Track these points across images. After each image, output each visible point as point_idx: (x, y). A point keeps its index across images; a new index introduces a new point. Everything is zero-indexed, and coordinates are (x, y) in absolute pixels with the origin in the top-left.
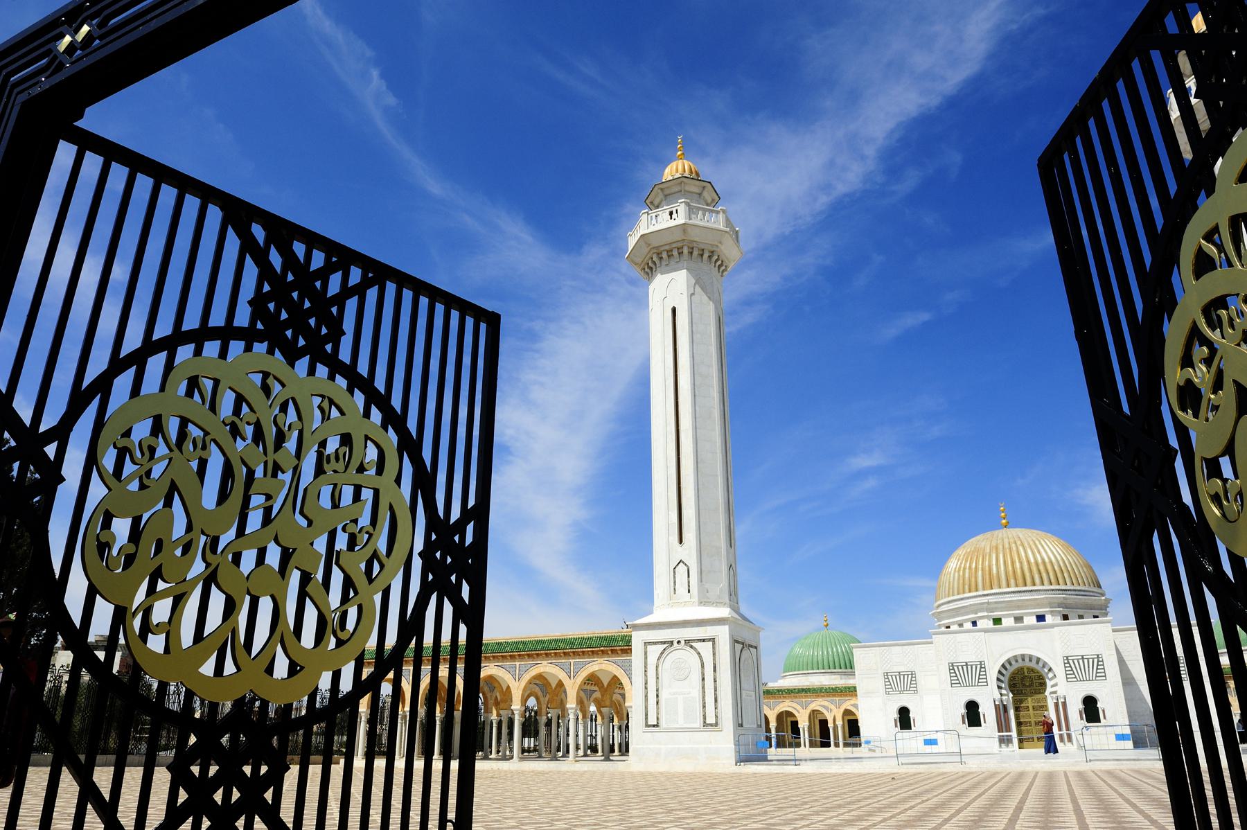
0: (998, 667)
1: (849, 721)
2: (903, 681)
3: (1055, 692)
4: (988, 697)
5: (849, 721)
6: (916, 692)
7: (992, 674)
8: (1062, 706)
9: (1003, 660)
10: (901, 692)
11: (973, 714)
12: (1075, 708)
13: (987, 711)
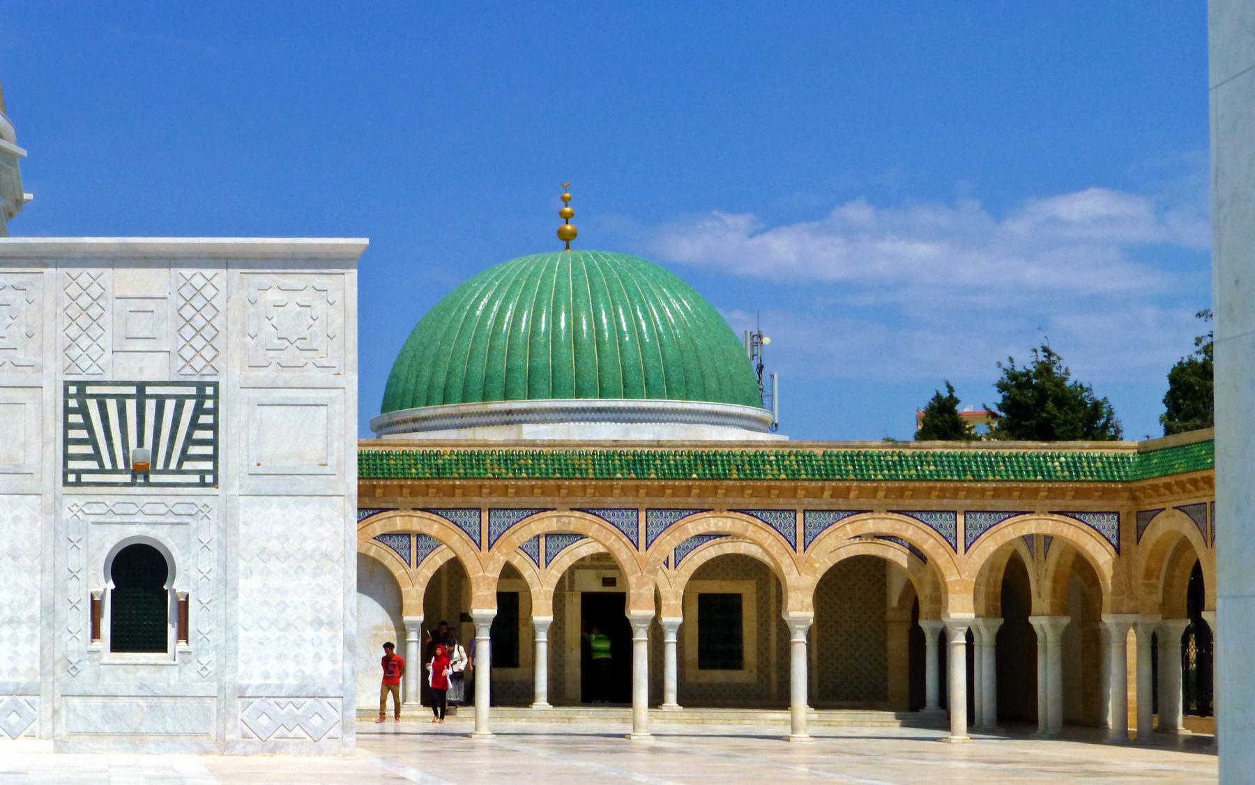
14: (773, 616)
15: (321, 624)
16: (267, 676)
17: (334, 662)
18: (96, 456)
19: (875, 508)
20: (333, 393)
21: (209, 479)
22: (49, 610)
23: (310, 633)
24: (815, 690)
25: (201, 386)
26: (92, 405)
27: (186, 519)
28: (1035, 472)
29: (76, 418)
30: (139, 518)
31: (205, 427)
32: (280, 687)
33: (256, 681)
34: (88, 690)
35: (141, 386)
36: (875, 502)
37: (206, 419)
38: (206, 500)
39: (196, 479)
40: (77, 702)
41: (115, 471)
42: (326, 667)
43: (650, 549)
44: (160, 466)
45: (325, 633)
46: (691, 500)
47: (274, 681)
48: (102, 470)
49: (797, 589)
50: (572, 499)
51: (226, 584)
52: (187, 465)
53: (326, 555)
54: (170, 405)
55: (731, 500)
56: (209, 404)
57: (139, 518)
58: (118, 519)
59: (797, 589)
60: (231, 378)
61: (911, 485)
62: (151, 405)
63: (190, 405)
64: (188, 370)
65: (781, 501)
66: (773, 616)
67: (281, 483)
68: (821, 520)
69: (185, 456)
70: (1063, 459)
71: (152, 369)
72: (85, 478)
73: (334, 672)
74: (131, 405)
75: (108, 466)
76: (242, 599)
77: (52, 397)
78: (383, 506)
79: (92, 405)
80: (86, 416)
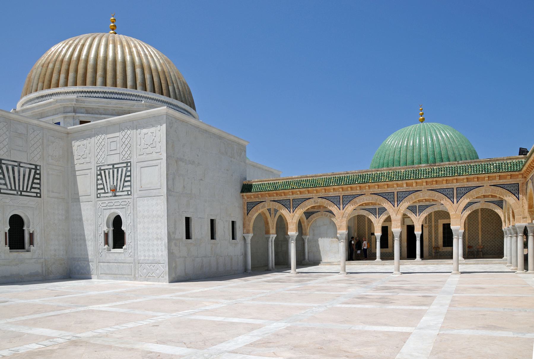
1: (387, 247)
5: (387, 247)
14: (467, 230)
15: (158, 239)
16: (145, 256)
17: (162, 252)
18: (103, 189)
19: (423, 189)
20: (159, 161)
21: (129, 193)
22: (95, 236)
23: (155, 242)
24: (472, 256)
25: (127, 163)
26: (103, 172)
27: (124, 206)
28: (482, 171)
29: (99, 177)
30: (114, 207)
31: (128, 176)
32: (148, 260)
33: (143, 258)
34: (104, 261)
35: (113, 165)
36: (423, 187)
37: (128, 174)
38: (129, 200)
39: (126, 193)
40: (102, 264)
41: (107, 193)
42: (160, 253)
43: (344, 210)
44: (118, 190)
45: (159, 242)
46: (358, 191)
47: (147, 258)
48: (105, 193)
49: (395, 220)
50: (318, 194)
51: (134, 227)
52: (125, 189)
53: (159, 216)
54: (120, 170)
55: (371, 190)
56: (129, 169)
57: (114, 207)
58: (109, 208)
59: (395, 220)
60: (134, 160)
61: (435, 179)
62: (116, 170)
63: (125, 169)
64: (124, 159)
65: (389, 189)
66: (467, 230)
67: (148, 193)
68: (403, 195)
69: (124, 186)
70: (495, 165)
71: (115, 159)
72: (102, 195)
73: (162, 255)
74: (111, 171)
75: (106, 191)
76: (138, 231)
77: (94, 172)
78: (262, 200)
79: (103, 172)
80: (102, 176)
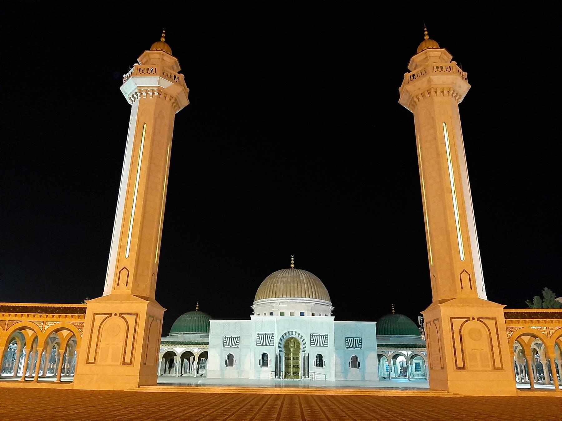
0: (280, 337)
2: (233, 341)
3: (304, 351)
4: (272, 352)
6: (238, 347)
7: (277, 340)
8: (306, 359)
9: (283, 333)
10: (231, 346)
11: (264, 361)
12: (313, 359)
13: (272, 359)
71: (354, 336)
